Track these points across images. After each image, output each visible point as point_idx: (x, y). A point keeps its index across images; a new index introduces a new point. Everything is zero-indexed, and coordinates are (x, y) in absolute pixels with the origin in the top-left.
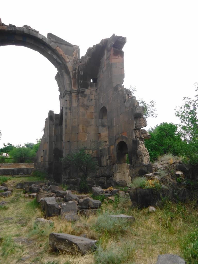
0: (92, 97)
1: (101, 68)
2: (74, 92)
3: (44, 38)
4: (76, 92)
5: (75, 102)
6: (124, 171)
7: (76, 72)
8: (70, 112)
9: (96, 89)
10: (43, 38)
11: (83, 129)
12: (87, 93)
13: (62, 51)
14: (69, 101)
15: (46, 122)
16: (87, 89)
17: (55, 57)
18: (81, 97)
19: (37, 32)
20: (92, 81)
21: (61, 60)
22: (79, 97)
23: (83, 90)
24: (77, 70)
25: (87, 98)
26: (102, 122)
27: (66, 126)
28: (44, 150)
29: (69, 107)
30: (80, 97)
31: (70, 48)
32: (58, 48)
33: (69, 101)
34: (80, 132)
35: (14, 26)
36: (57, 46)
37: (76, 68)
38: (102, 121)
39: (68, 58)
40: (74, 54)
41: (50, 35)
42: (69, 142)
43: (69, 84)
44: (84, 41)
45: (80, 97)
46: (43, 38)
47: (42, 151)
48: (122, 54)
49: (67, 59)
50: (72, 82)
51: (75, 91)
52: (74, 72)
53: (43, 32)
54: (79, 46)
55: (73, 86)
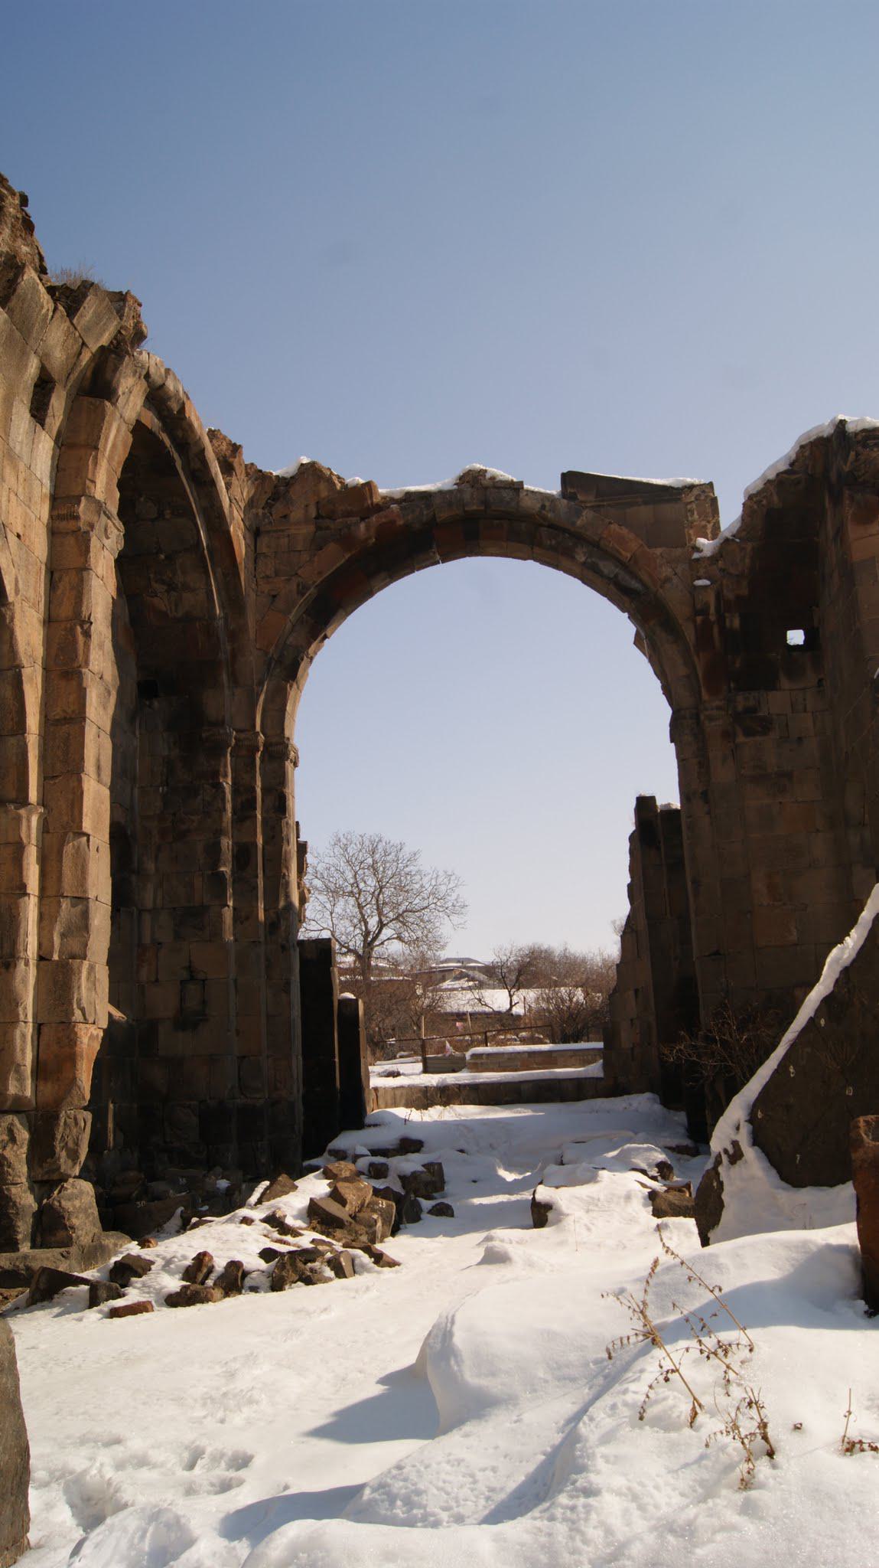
2: (711, 719)
3: (547, 504)
8: (709, 813)
9: (820, 680)
10: (543, 507)
13: (632, 536)
15: (631, 852)
17: (608, 568)
18: (749, 732)
19: (516, 487)
24: (712, 610)
28: (636, 991)
30: (741, 739)
31: (668, 510)
32: (614, 527)
37: (707, 605)
41: (570, 479)
42: (717, 953)
47: (631, 993)
52: (699, 619)
54: (711, 485)
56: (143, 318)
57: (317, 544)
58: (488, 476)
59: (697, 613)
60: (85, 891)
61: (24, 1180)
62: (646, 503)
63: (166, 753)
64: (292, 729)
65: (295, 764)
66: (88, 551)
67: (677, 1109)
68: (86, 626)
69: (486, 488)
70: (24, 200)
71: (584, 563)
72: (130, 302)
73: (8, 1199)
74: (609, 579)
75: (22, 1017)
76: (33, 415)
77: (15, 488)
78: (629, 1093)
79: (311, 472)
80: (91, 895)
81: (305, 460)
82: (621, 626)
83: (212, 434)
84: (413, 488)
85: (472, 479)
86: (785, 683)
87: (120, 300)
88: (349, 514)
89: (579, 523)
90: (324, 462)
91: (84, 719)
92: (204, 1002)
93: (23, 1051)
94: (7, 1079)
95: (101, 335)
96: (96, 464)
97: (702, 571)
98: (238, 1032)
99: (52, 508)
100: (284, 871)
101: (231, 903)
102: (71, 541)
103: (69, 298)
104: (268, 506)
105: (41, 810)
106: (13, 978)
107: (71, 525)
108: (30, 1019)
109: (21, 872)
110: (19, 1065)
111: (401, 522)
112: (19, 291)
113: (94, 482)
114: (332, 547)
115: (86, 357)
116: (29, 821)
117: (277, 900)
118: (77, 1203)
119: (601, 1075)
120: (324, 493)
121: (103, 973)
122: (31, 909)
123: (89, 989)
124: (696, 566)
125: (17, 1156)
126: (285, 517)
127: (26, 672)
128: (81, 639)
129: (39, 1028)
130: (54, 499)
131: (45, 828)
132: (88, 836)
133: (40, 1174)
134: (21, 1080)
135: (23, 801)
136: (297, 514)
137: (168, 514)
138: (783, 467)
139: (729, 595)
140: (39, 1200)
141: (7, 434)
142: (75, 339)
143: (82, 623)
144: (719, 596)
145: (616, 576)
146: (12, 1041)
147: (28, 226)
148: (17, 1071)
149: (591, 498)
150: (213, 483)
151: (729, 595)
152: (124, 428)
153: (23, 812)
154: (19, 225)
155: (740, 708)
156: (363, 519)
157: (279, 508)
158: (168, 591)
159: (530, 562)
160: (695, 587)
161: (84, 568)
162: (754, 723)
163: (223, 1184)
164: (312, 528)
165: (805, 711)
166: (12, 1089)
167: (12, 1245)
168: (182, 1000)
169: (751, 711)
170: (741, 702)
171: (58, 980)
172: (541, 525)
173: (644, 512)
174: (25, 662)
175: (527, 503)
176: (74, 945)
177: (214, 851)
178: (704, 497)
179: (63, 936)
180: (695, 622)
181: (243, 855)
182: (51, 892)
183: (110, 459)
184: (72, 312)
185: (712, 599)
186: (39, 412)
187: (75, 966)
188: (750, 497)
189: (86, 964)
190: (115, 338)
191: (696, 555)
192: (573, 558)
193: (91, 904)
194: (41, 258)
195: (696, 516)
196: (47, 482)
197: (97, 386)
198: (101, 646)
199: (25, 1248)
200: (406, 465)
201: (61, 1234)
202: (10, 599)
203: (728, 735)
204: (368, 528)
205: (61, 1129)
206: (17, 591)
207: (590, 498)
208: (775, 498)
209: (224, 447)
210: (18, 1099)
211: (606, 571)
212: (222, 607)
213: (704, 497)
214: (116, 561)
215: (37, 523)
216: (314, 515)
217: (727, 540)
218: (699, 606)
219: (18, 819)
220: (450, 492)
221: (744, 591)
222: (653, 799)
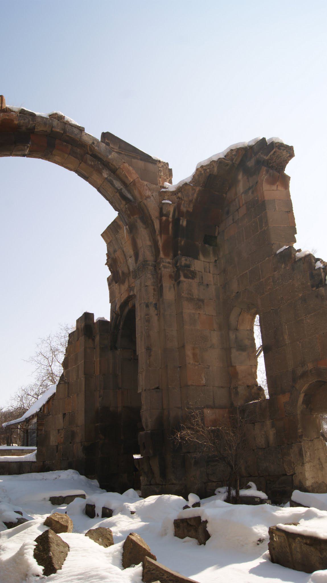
0: (209, 278)
1: (228, 213)
2: (165, 267)
3: (95, 142)
4: (171, 266)
5: (170, 288)
6: (319, 459)
7: (167, 220)
8: (157, 315)
9: (216, 261)
10: (93, 143)
11: (194, 355)
12: (197, 269)
13: (134, 171)
14: (153, 287)
16: (195, 260)
17: (118, 184)
18: (186, 276)
19: (81, 130)
21: (130, 191)
22: (179, 277)
23: (188, 263)
24: (171, 216)
25: (197, 280)
26: (236, 338)
27: (149, 349)
28: (64, 415)
29: (154, 303)
31: (150, 166)
32: (126, 165)
33: (153, 287)
34: (189, 363)
35: (32, 115)
36: (123, 161)
38: (236, 335)
39: (147, 188)
40: (160, 179)
41: (106, 136)
42: (158, 388)
43: (151, 246)
44: (183, 154)
45: (182, 278)
46: (93, 143)
47: (60, 416)
48: (285, 181)
49: (146, 190)
50: (160, 244)
51: (167, 265)
53: (94, 131)
55: (161, 252)
62: (141, 160)
67: (92, 478)
69: (66, 124)
71: (106, 179)
74: (117, 189)
78: (52, 470)
84: (26, 109)
85: (57, 117)
89: (110, 157)
97: (166, 197)
111: (16, 122)
119: (35, 460)
124: (163, 194)
138: (222, 156)
145: (121, 189)
149: (117, 148)
151: (184, 209)
155: (183, 264)
165: (210, 272)
169: (188, 266)
172: (88, 153)
173: (141, 164)
175: (85, 138)
178: (161, 170)
185: (172, 210)
191: (163, 190)
192: (101, 174)
195: (162, 174)
208: (216, 169)
211: (116, 186)
220: (47, 118)
221: (191, 210)
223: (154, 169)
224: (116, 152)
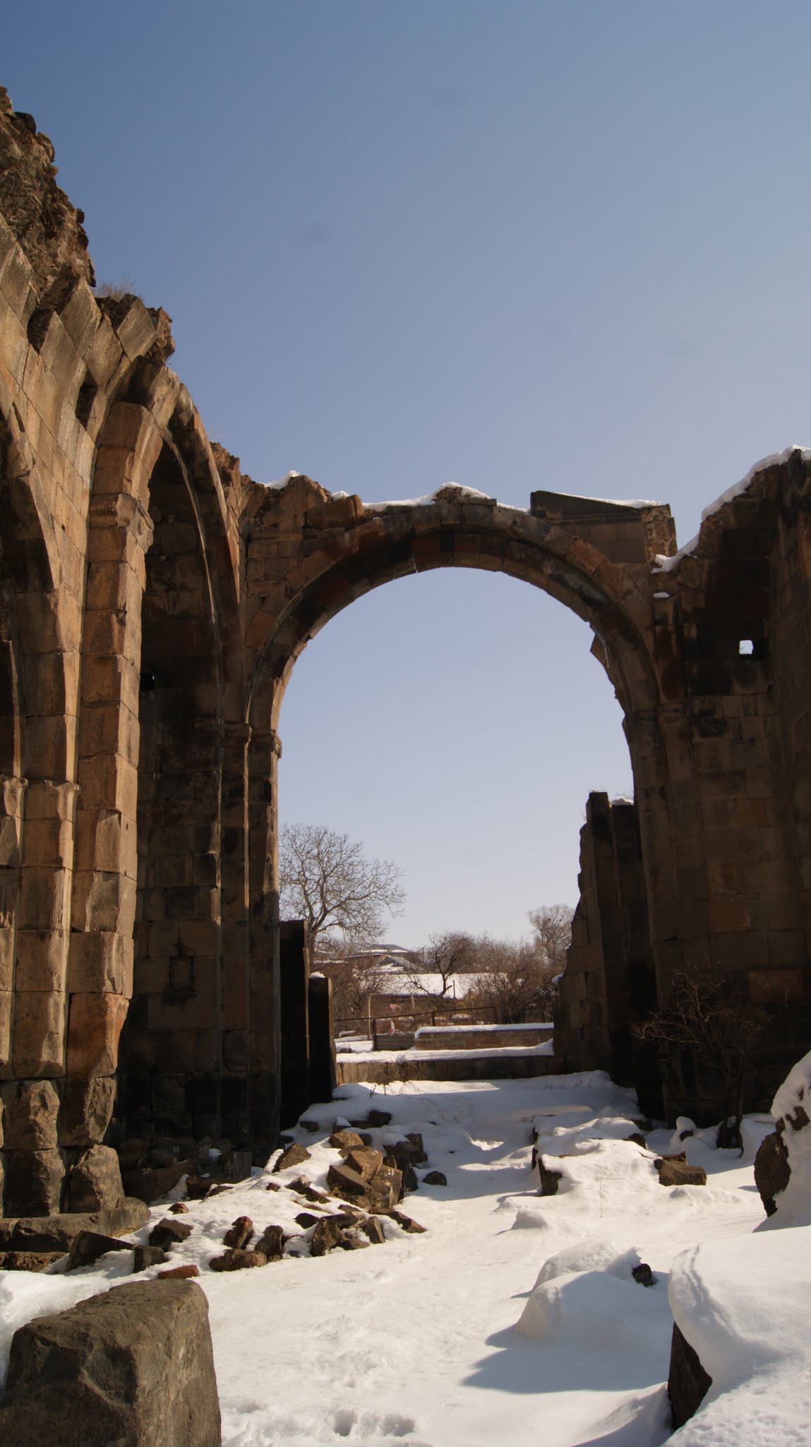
3: (518, 520)
9: (770, 687)
10: (515, 523)
15: (583, 844)
17: (572, 580)
18: (704, 734)
19: (490, 504)
20: (746, 647)
24: (671, 621)
28: (586, 974)
30: (697, 739)
32: (580, 543)
37: (665, 616)
42: (675, 938)
45: (697, 739)
47: (581, 976)
52: (658, 628)
53: (514, 500)
54: (667, 507)
56: (173, 333)
57: (305, 552)
58: (464, 493)
59: (656, 622)
60: (116, 866)
61: (54, 1145)
62: (609, 522)
63: (160, 742)
64: (276, 721)
65: (279, 756)
66: (123, 544)
67: (627, 1086)
68: (121, 615)
69: (462, 504)
70: (81, 217)
71: (551, 575)
72: (162, 318)
73: (40, 1164)
75: (56, 987)
76: (78, 417)
77: (61, 481)
78: (578, 1071)
79: (300, 486)
80: (122, 870)
81: (295, 474)
82: (584, 633)
83: (213, 445)
84: (394, 503)
85: (449, 496)
86: (737, 688)
87: (155, 314)
88: (333, 525)
89: (548, 538)
90: (312, 477)
91: (118, 702)
92: (192, 978)
93: (56, 1019)
94: (40, 1047)
95: (139, 346)
96: (132, 463)
97: (661, 585)
98: (223, 1007)
99: (91, 504)
100: (268, 855)
101: (219, 885)
102: (107, 534)
103: (116, 309)
104: (260, 515)
105: (77, 788)
106: (47, 948)
107: (107, 520)
108: (63, 988)
109: (57, 850)
110: (52, 1033)
111: (382, 534)
112: (74, 299)
113: (130, 481)
114: (318, 555)
115: (125, 366)
116: (65, 798)
117: (262, 884)
118: (104, 1169)
119: (551, 1053)
120: (312, 505)
121: (129, 945)
122: (65, 881)
123: (118, 961)
124: (656, 580)
125: (48, 1122)
126: (275, 525)
127: (67, 656)
128: (116, 626)
129: (70, 997)
130: (93, 495)
131: (79, 805)
132: (120, 813)
133: (69, 1140)
134: (53, 1047)
135: (61, 779)
136: (286, 523)
137: (171, 518)
138: (739, 491)
139: (687, 607)
140: (67, 1166)
141: (57, 432)
142: (117, 349)
143: (118, 612)
144: (677, 607)
145: (581, 588)
146: (46, 1010)
147: (83, 240)
148: (51, 1039)
149: (559, 516)
150: (214, 491)
151: (687, 607)
152: (157, 432)
153: (60, 789)
154: (75, 240)
155: (696, 711)
156: (347, 530)
157: (269, 518)
158: (166, 591)
159: (500, 574)
160: (655, 599)
161: (120, 561)
162: (711, 725)
163: (215, 1153)
164: (300, 536)
165: (756, 715)
166: (45, 1056)
167: (43, 1210)
168: (171, 975)
170: (697, 705)
171: (90, 950)
173: (608, 530)
174: (65, 647)
175: (499, 518)
176: (105, 918)
177: (204, 836)
178: (659, 520)
179: (94, 909)
180: (654, 631)
181: (231, 840)
182: (84, 866)
183: (144, 461)
184: (116, 323)
185: (670, 609)
186: (83, 413)
187: (107, 938)
188: (708, 518)
189: (116, 935)
190: (151, 349)
191: (655, 570)
193: (121, 878)
194: (92, 272)
195: (654, 534)
196: (88, 480)
197: (135, 390)
198: (133, 635)
199: (55, 1213)
200: (389, 483)
201: (89, 1200)
202: (56, 586)
203: (685, 736)
204: (352, 539)
205: (90, 1096)
206: (61, 580)
207: (558, 516)
208: (732, 519)
209: (223, 459)
210: (50, 1066)
211: (571, 584)
212: (217, 607)
213: (661, 519)
214: (146, 556)
215: (78, 517)
216: (302, 524)
217: (685, 557)
218: (658, 617)
219: (56, 795)
220: (429, 507)
222: (605, 795)
223: (643, 525)
224: (558, 524)
